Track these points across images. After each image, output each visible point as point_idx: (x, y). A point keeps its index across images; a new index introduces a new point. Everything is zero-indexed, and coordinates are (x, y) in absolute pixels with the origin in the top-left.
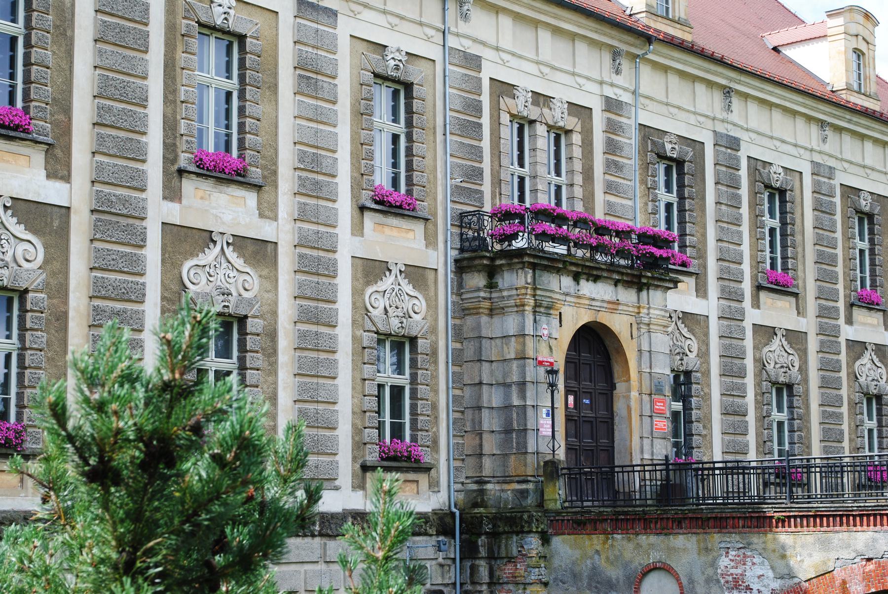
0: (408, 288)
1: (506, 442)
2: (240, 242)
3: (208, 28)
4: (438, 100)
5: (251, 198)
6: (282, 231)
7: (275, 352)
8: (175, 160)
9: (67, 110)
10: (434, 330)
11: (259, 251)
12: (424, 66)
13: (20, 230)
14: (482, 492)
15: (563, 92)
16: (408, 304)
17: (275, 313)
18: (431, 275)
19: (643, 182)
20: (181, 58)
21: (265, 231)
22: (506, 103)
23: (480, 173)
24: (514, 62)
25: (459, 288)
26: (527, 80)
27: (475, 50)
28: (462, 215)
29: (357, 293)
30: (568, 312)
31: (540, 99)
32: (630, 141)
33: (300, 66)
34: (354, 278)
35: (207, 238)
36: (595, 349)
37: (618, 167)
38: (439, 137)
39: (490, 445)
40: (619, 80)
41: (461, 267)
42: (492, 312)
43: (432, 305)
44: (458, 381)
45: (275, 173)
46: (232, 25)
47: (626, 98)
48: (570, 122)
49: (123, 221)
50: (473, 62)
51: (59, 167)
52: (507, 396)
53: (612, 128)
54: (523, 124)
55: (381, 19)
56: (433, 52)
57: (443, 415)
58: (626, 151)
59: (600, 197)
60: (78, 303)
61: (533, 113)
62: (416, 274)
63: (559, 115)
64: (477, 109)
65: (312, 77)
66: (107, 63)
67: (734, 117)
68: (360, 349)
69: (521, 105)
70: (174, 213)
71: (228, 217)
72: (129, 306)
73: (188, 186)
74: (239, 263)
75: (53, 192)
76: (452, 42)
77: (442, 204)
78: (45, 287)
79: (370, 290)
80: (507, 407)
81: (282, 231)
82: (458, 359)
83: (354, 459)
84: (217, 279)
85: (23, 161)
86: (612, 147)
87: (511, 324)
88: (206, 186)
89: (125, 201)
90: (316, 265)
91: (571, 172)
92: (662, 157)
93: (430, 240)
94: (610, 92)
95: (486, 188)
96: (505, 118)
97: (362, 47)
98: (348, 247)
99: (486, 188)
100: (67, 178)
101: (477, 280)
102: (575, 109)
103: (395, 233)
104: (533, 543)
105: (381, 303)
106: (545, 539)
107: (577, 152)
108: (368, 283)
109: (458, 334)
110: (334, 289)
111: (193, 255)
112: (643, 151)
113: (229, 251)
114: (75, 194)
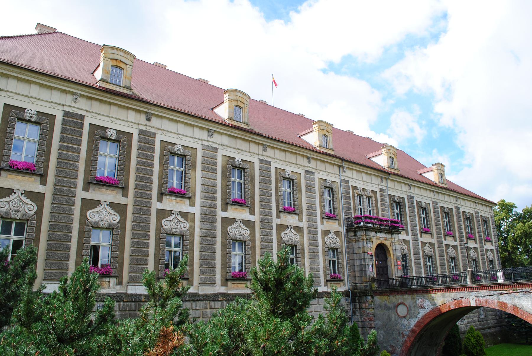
0: (335, 237)
1: (362, 273)
2: (295, 228)
3: (285, 178)
4: (340, 191)
5: (297, 217)
6: (304, 224)
7: (304, 253)
8: (279, 209)
9: (254, 199)
10: (342, 247)
11: (299, 230)
12: (335, 184)
13: (244, 227)
14: (356, 286)
15: (369, 187)
16: (335, 241)
17: (303, 244)
18: (340, 233)
19: (391, 208)
20: (279, 185)
21: (300, 224)
22: (356, 191)
23: (351, 208)
24: (357, 181)
25: (347, 236)
27: (348, 179)
28: (347, 219)
29: (323, 238)
30: (374, 241)
31: (364, 190)
32: (387, 198)
33: (307, 185)
34: (322, 235)
35: (287, 227)
36: (382, 249)
37: (384, 205)
38: (340, 200)
39: (357, 274)
40: (383, 184)
41: (348, 231)
42: (356, 242)
43: (341, 241)
44: (348, 259)
45: (302, 211)
46: (290, 177)
47: (385, 188)
48: (372, 195)
49: (267, 224)
50: (347, 182)
51: (252, 213)
52: (361, 262)
53: (382, 195)
54: (360, 196)
55: (325, 173)
56: (337, 180)
57: (345, 267)
58: (386, 201)
59: (380, 212)
60: (258, 243)
61: (362, 193)
62: (337, 233)
63: (369, 193)
64: (349, 193)
65: (310, 188)
66: (262, 188)
67: (412, 191)
68: (324, 252)
69: (359, 191)
70: (279, 221)
71: (291, 222)
72: (269, 244)
73: (282, 215)
74: (294, 232)
75: (251, 218)
76: (342, 178)
77: (342, 216)
78: (250, 240)
79: (326, 238)
80: (361, 265)
81: (304, 224)
82: (348, 253)
83: (324, 279)
84: (289, 236)
85: (244, 211)
86: (382, 200)
87: (361, 244)
88: (286, 215)
89: (268, 219)
90: (313, 232)
91: (373, 207)
92: (395, 202)
93: (340, 225)
94: (381, 187)
95: (352, 211)
96: (356, 195)
97: (321, 180)
99: (352, 211)
100: (254, 215)
101: (352, 234)
102: (373, 192)
103: (331, 223)
104: (370, 298)
105: (329, 241)
106: (373, 297)
107: (374, 202)
108: (325, 236)
109: (348, 247)
110: (317, 237)
111: (284, 231)
112: (390, 200)
113: (292, 230)
114: (256, 218)
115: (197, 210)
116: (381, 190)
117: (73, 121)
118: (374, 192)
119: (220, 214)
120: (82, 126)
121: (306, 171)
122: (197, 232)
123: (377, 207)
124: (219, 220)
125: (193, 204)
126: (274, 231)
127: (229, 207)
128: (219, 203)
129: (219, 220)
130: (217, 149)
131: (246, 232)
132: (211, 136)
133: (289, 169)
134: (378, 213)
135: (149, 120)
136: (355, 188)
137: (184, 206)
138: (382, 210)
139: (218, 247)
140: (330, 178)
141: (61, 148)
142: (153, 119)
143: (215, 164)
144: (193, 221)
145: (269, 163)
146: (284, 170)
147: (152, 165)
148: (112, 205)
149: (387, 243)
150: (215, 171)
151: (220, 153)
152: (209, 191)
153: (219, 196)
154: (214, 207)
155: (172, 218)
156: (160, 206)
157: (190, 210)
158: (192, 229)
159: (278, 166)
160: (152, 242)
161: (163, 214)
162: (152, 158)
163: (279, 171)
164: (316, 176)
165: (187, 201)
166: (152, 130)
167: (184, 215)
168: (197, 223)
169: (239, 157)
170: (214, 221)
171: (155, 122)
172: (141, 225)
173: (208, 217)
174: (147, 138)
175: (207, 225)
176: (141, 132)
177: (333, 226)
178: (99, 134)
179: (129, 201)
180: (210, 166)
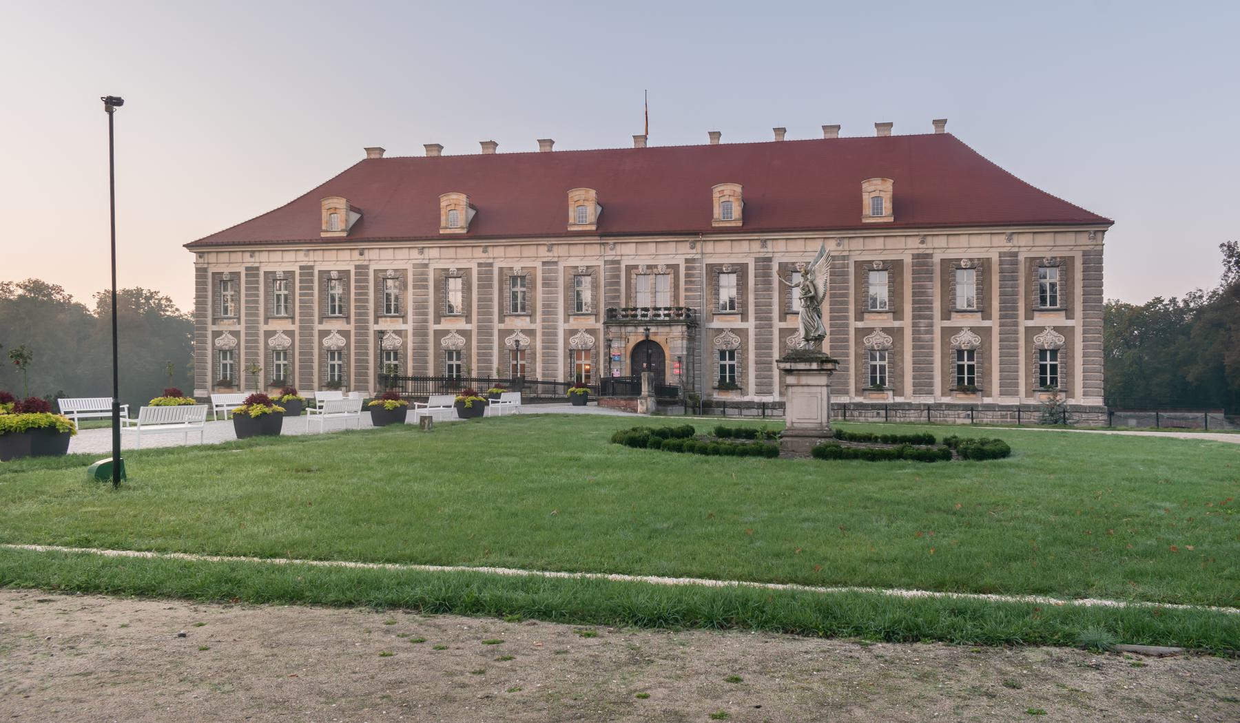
5: (528, 319)
15: (661, 262)
19: (709, 284)
21: (533, 326)
23: (618, 297)
26: (642, 262)
31: (649, 267)
32: (701, 273)
37: (691, 282)
59: (682, 294)
60: (474, 351)
62: (592, 332)
64: (618, 277)
67: (770, 249)
70: (502, 326)
77: (602, 309)
81: (538, 326)
90: (550, 334)
93: (597, 321)
94: (689, 257)
98: (562, 327)
102: (668, 266)
114: (473, 327)
115: (409, 327)
116: (687, 261)
117: (307, 271)
118: (675, 268)
119: (432, 327)
120: (312, 274)
121: (544, 263)
122: (410, 346)
123: (676, 286)
125: (405, 322)
126: (496, 337)
128: (431, 317)
132: (422, 253)
133: (517, 267)
135: (361, 254)
137: (399, 325)
138: (686, 290)
139: (431, 359)
140: (582, 264)
141: (301, 295)
142: (366, 252)
143: (426, 280)
144: (406, 336)
145: (491, 265)
146: (511, 268)
147: (366, 294)
148: (339, 332)
150: (426, 287)
151: (433, 266)
152: (421, 308)
153: (431, 310)
154: (426, 321)
157: (403, 327)
158: (404, 345)
159: (503, 265)
160: (371, 358)
162: (366, 287)
163: (505, 271)
165: (401, 320)
168: (410, 339)
169: (452, 267)
170: (426, 335)
171: (369, 255)
173: (421, 332)
174: (362, 270)
176: (357, 267)
177: (590, 322)
178: (325, 277)
179: (351, 327)
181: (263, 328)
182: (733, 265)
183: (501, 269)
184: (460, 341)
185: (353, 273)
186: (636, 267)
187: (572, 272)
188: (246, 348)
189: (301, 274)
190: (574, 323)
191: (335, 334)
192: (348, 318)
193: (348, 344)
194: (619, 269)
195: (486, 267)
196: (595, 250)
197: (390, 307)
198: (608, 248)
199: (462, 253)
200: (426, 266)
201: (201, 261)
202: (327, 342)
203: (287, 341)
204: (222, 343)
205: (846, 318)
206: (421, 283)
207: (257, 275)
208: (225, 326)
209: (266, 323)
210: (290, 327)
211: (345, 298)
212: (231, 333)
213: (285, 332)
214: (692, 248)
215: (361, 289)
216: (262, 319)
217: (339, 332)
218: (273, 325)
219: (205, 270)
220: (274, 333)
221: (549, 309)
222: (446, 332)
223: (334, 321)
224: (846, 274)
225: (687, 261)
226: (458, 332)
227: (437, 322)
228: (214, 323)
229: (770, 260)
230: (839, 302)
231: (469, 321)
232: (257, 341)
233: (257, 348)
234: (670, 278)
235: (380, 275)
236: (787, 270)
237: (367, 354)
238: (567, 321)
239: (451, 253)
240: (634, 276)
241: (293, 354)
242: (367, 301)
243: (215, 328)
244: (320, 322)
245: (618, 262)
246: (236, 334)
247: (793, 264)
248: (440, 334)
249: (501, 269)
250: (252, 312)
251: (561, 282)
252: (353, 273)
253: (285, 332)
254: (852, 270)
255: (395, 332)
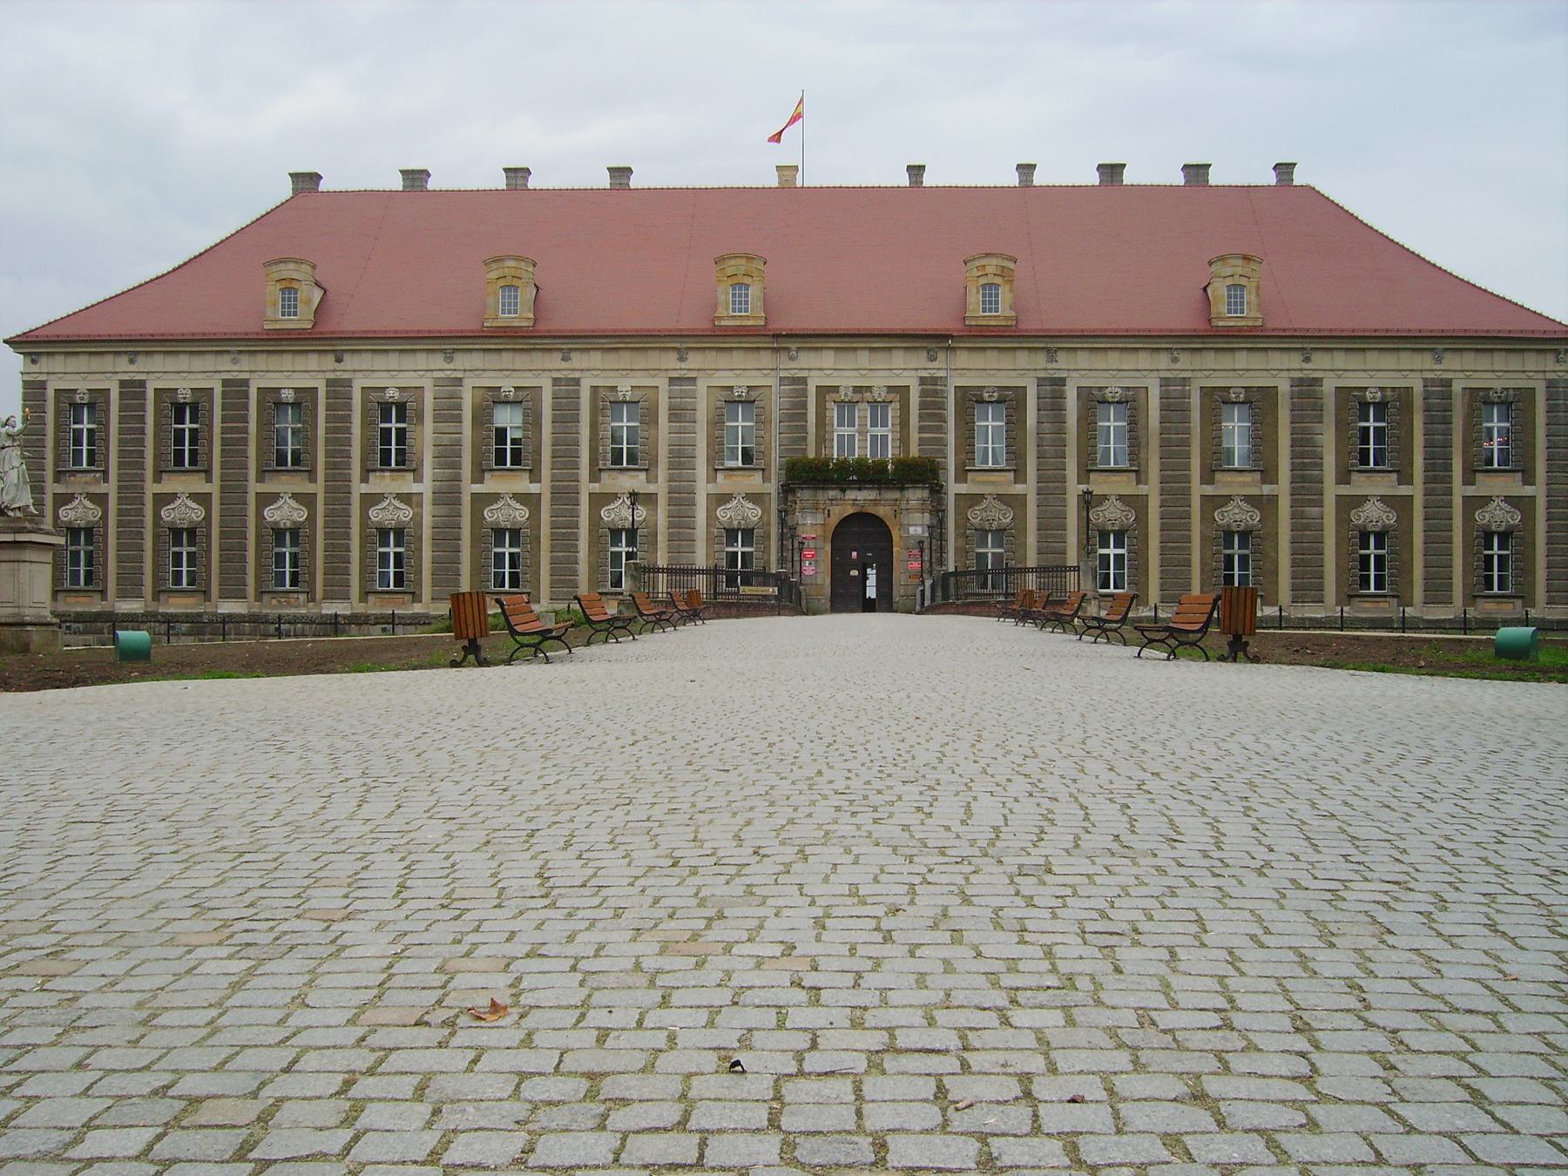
0: (751, 505)
5: (643, 476)
13: (518, 506)
21: (651, 488)
24: (836, 373)
26: (846, 381)
31: (858, 389)
40: (935, 365)
43: (766, 511)
59: (914, 436)
60: (545, 530)
61: (857, 397)
62: (755, 498)
63: (880, 394)
64: (804, 405)
70: (596, 487)
73: (604, 475)
76: (783, 374)
77: (775, 460)
81: (660, 487)
82: (782, 538)
90: (681, 501)
93: (766, 479)
94: (925, 374)
98: (702, 490)
102: (891, 389)
114: (542, 488)
115: (425, 488)
116: (923, 381)
117: (236, 389)
119: (469, 488)
122: (427, 520)
123: (904, 423)
124: (466, 500)
125: (418, 479)
127: (487, 475)
129: (466, 500)
130: (460, 379)
131: (521, 514)
132: (450, 360)
134: (904, 440)
135: (339, 360)
136: (822, 391)
137: (407, 484)
142: (347, 357)
145: (577, 382)
147: (348, 430)
148: (295, 496)
149: (882, 511)
150: (458, 419)
151: (469, 383)
152: (448, 456)
155: (384, 504)
156: (365, 489)
157: (415, 488)
158: (417, 520)
161: (370, 500)
163: (602, 393)
164: (701, 387)
166: (346, 375)
167: (406, 498)
168: (427, 508)
169: (507, 385)
170: (457, 502)
171: (350, 362)
172: (338, 521)
173: (447, 496)
175: (444, 510)
177: (754, 482)
178: (272, 402)
179: (319, 488)
180: (449, 413)
181: (151, 488)
182: (1001, 388)
183: (595, 389)
184: (521, 514)
185: (322, 393)
186: (835, 389)
187: (724, 395)
188: (120, 524)
189: (224, 395)
190: (723, 483)
191: (186, 497)
192: (312, 474)
193: (312, 519)
194: (804, 393)
195: (567, 388)
196: (766, 359)
197: (392, 452)
198: (784, 355)
199: (521, 361)
200: (458, 382)
201: (35, 368)
202: (272, 514)
203: (196, 513)
204: (71, 515)
205: (1187, 479)
206: (449, 413)
207: (143, 395)
208: (76, 485)
209: (157, 479)
210: (204, 488)
211: (306, 436)
212: (92, 497)
213: (194, 497)
214: (933, 359)
215: (339, 422)
216: (149, 473)
217: (295, 496)
218: (170, 485)
219: (42, 385)
220: (174, 496)
221: (681, 459)
222: (496, 497)
223: (283, 478)
224: (1185, 409)
225: (923, 381)
226: (516, 496)
227: (478, 478)
228: (57, 480)
229: (1061, 382)
230: (1174, 451)
231: (535, 476)
232: (140, 512)
233: (141, 524)
234: (892, 412)
235: (374, 396)
236: (1093, 401)
237: (347, 536)
238: (711, 479)
239: (506, 360)
240: (831, 405)
241: (209, 536)
242: (348, 442)
243: (60, 489)
244: (260, 479)
245: (803, 381)
246: (100, 499)
247: (1100, 388)
248: (481, 501)
249: (595, 389)
250: (131, 460)
251: (702, 415)
252: (322, 393)
253: (194, 497)
254: (1195, 400)
255: (399, 496)
